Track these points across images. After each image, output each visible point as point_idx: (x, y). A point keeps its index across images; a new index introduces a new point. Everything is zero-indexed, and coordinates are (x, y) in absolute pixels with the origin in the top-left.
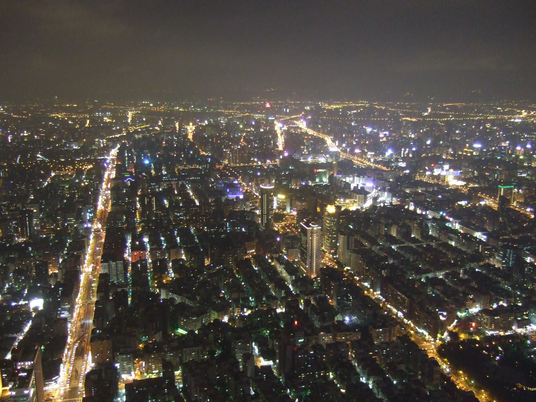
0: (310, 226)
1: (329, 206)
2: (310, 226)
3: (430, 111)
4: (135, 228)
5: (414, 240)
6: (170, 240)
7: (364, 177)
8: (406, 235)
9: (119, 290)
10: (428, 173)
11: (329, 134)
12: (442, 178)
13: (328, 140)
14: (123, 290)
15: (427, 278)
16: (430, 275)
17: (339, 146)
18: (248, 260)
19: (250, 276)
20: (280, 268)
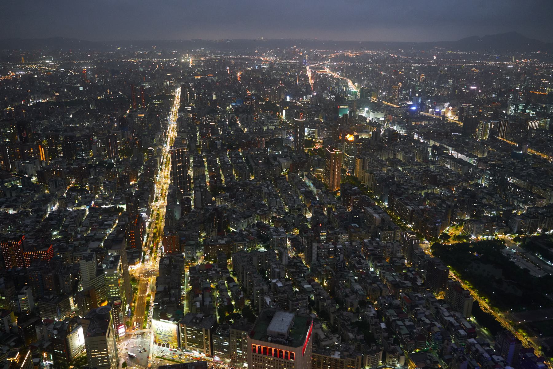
0: (334, 151)
1: (348, 135)
2: (334, 151)
3: (435, 58)
5: (417, 164)
10: (431, 110)
11: (350, 78)
12: (442, 114)
14: (187, 198)
15: (426, 193)
16: (429, 191)
17: (358, 87)
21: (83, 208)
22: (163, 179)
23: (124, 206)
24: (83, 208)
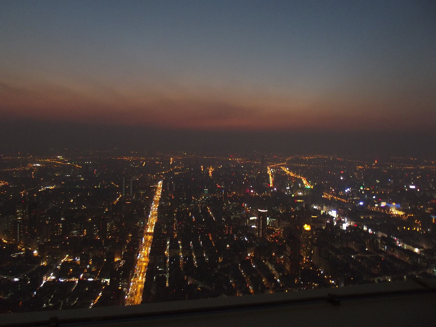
4: (173, 235)
6: (196, 243)
9: (160, 275)
13: (305, 182)
15: (379, 281)
18: (249, 260)
19: (249, 270)
20: (271, 267)
21: (73, 279)
24: (73, 279)
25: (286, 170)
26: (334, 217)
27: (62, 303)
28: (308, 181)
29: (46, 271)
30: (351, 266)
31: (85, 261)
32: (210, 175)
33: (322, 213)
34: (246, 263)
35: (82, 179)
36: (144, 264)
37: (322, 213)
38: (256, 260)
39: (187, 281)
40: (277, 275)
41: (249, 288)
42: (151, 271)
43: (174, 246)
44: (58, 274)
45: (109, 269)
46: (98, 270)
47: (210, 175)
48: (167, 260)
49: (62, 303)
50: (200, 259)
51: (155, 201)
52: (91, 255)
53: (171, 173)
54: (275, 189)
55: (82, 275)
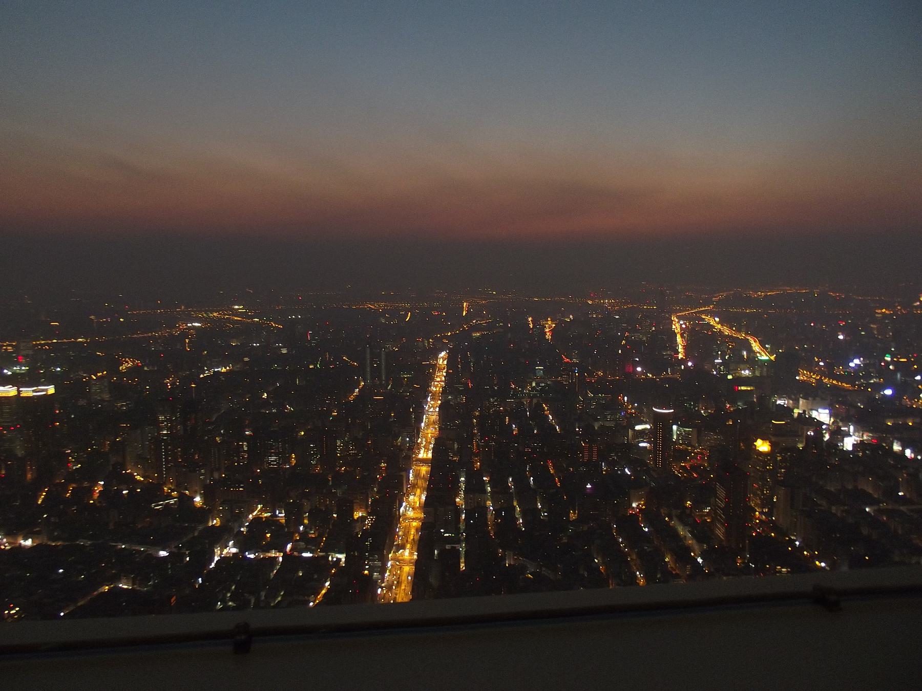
4: (473, 463)
6: (521, 481)
7: (814, 399)
8: (891, 493)
13: (756, 347)
19: (635, 538)
21: (273, 554)
22: (412, 509)
23: (342, 557)
24: (273, 554)
25: (714, 322)
26: (824, 424)
27: (253, 601)
28: (762, 344)
29: (219, 536)
30: (865, 531)
31: (294, 516)
32: (548, 336)
33: (796, 415)
34: (629, 524)
35: (284, 351)
36: (414, 524)
37: (796, 415)
38: (649, 515)
39: (503, 559)
40: (696, 547)
41: (636, 576)
42: (427, 541)
43: (475, 487)
44: (244, 544)
45: (342, 534)
46: (320, 536)
47: (548, 336)
48: (460, 516)
49: (253, 601)
50: (530, 513)
51: (434, 394)
52: (307, 505)
53: (467, 335)
54: (690, 364)
55: (289, 546)
